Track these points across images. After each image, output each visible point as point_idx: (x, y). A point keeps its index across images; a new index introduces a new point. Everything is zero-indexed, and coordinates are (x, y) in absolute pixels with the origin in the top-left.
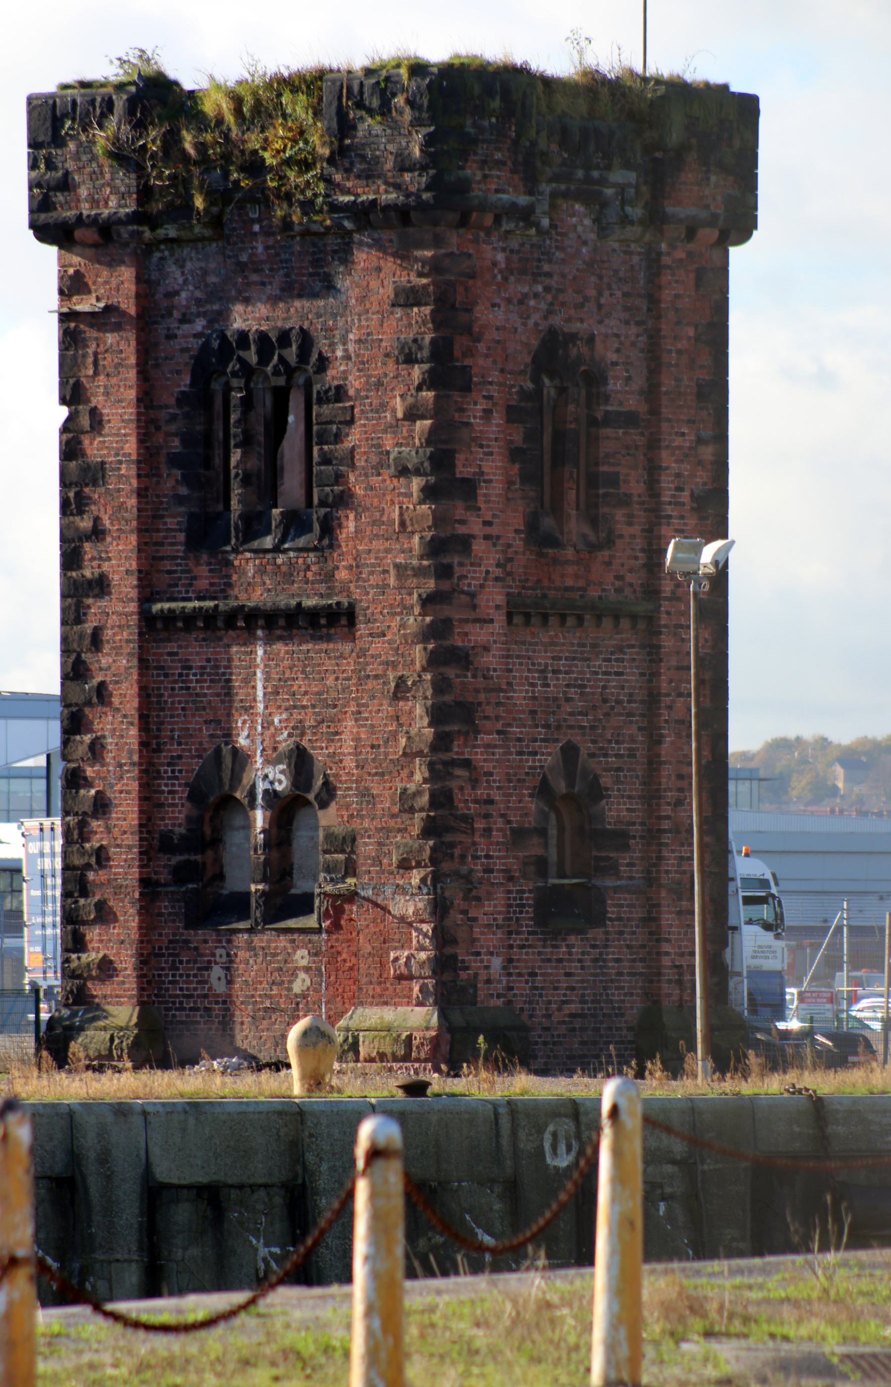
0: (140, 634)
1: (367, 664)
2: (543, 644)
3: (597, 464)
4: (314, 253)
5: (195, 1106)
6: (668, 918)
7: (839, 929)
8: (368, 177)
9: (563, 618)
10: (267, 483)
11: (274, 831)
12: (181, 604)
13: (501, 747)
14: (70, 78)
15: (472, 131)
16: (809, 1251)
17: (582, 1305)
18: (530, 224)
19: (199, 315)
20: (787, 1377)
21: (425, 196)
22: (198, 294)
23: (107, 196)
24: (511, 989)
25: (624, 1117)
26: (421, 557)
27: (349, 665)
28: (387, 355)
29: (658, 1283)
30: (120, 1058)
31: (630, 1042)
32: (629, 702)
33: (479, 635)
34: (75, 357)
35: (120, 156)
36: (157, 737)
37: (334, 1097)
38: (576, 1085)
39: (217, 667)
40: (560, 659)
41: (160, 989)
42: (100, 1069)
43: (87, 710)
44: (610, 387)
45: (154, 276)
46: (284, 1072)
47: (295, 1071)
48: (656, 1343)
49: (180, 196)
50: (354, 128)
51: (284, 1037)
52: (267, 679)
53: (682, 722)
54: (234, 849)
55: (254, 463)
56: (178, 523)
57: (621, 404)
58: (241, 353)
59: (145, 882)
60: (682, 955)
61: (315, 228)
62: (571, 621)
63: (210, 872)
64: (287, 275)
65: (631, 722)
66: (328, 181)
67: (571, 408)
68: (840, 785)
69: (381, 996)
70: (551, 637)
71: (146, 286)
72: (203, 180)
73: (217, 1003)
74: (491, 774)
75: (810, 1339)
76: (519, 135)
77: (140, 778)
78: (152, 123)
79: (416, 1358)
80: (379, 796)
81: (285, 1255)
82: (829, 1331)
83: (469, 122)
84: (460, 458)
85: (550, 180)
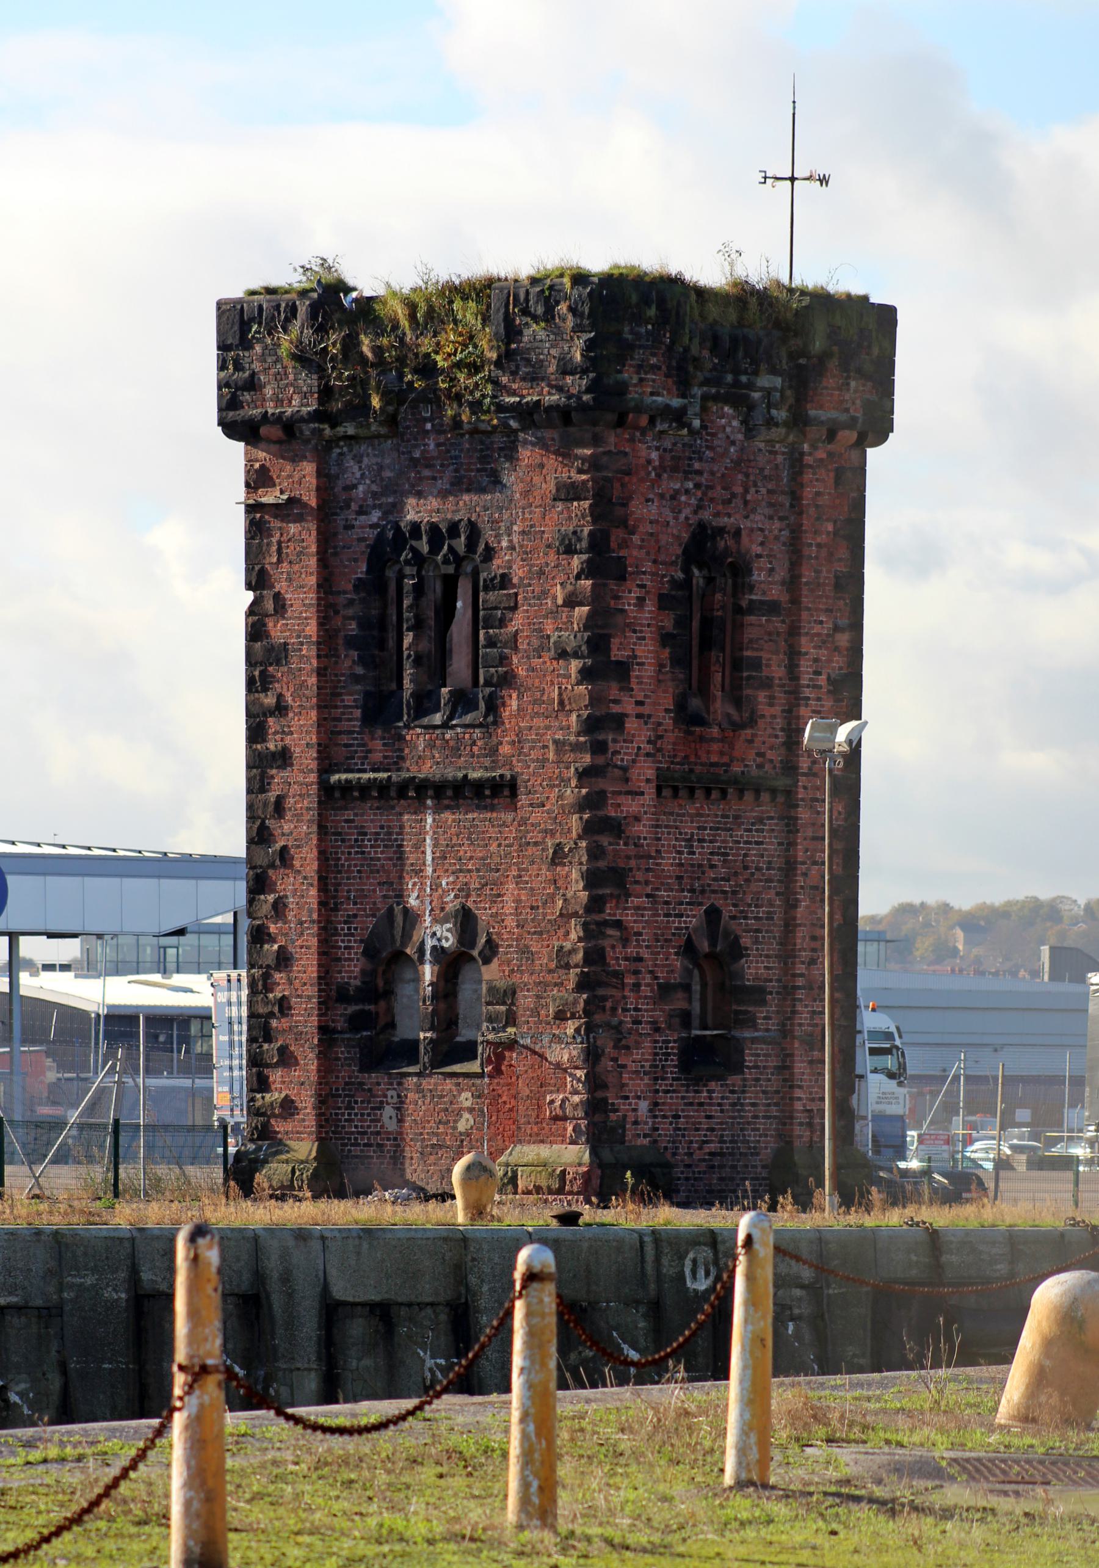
0: (319, 802)
1: (528, 832)
2: (689, 815)
3: (741, 649)
4: (482, 450)
5: (368, 1232)
6: (800, 1067)
7: (956, 1078)
8: (533, 380)
9: (708, 791)
10: (436, 664)
11: (442, 984)
12: (357, 775)
13: (650, 909)
14: (256, 284)
15: (630, 337)
16: (923, 1367)
17: (720, 1411)
18: (682, 425)
19: (374, 507)
20: (900, 1478)
21: (585, 398)
22: (374, 488)
23: (292, 395)
24: (657, 1129)
25: (756, 1246)
26: (578, 734)
27: (511, 833)
28: (549, 546)
29: (786, 1395)
30: (300, 1188)
31: (764, 1179)
32: (768, 869)
33: (631, 806)
34: (260, 545)
35: (301, 358)
36: (335, 897)
37: (495, 1225)
38: (714, 1217)
39: (390, 834)
40: (705, 829)
41: (337, 1126)
42: (282, 1198)
43: (271, 872)
44: (755, 577)
45: (334, 470)
46: (449, 1202)
47: (459, 1202)
48: (784, 1448)
49: (358, 396)
50: (520, 333)
51: (450, 1171)
52: (435, 845)
53: (816, 888)
54: (405, 1000)
55: (425, 646)
56: (355, 700)
57: (764, 593)
58: (414, 543)
59: (323, 1029)
60: (813, 1100)
61: (483, 427)
62: (715, 794)
63: (382, 1022)
64: (456, 471)
65: (770, 887)
66: (495, 383)
67: (718, 596)
68: (961, 947)
69: (538, 1135)
70: (697, 809)
71: (326, 479)
72: (380, 382)
73: (389, 1139)
74: (640, 934)
75: (922, 1445)
76: (673, 342)
77: (319, 935)
78: (332, 327)
79: (566, 1458)
80: (537, 953)
81: (450, 1367)
82: (939, 1438)
83: (627, 329)
84: (615, 642)
85: (702, 385)
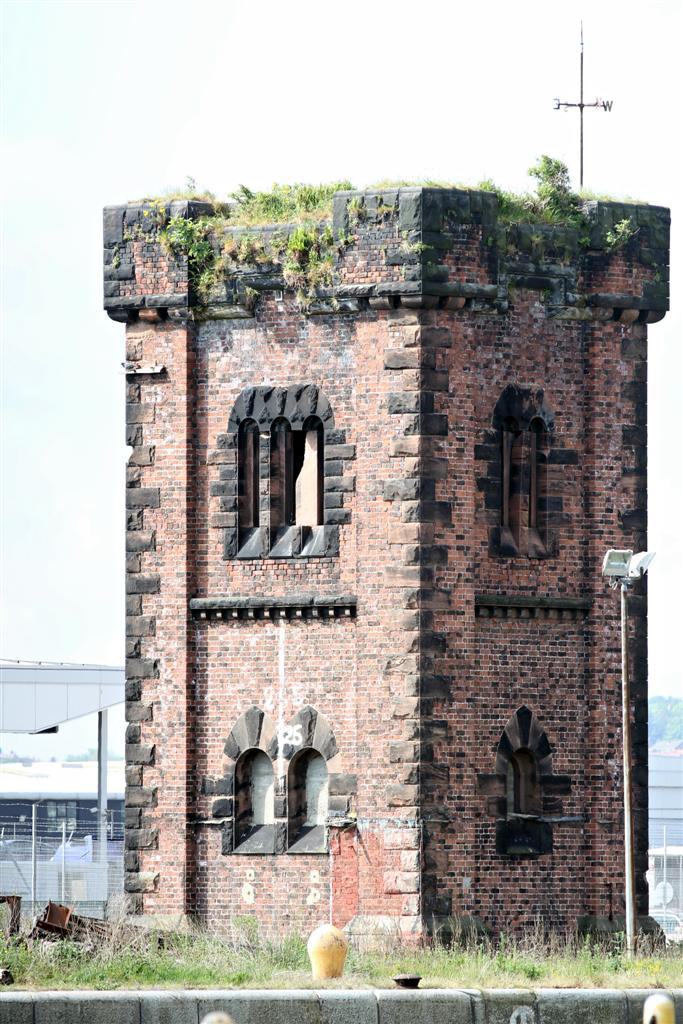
3: (544, 491)
6: (601, 846)
11: (293, 777)
52: (287, 658)
57: (563, 445)
62: (524, 613)
77: (188, 735)
